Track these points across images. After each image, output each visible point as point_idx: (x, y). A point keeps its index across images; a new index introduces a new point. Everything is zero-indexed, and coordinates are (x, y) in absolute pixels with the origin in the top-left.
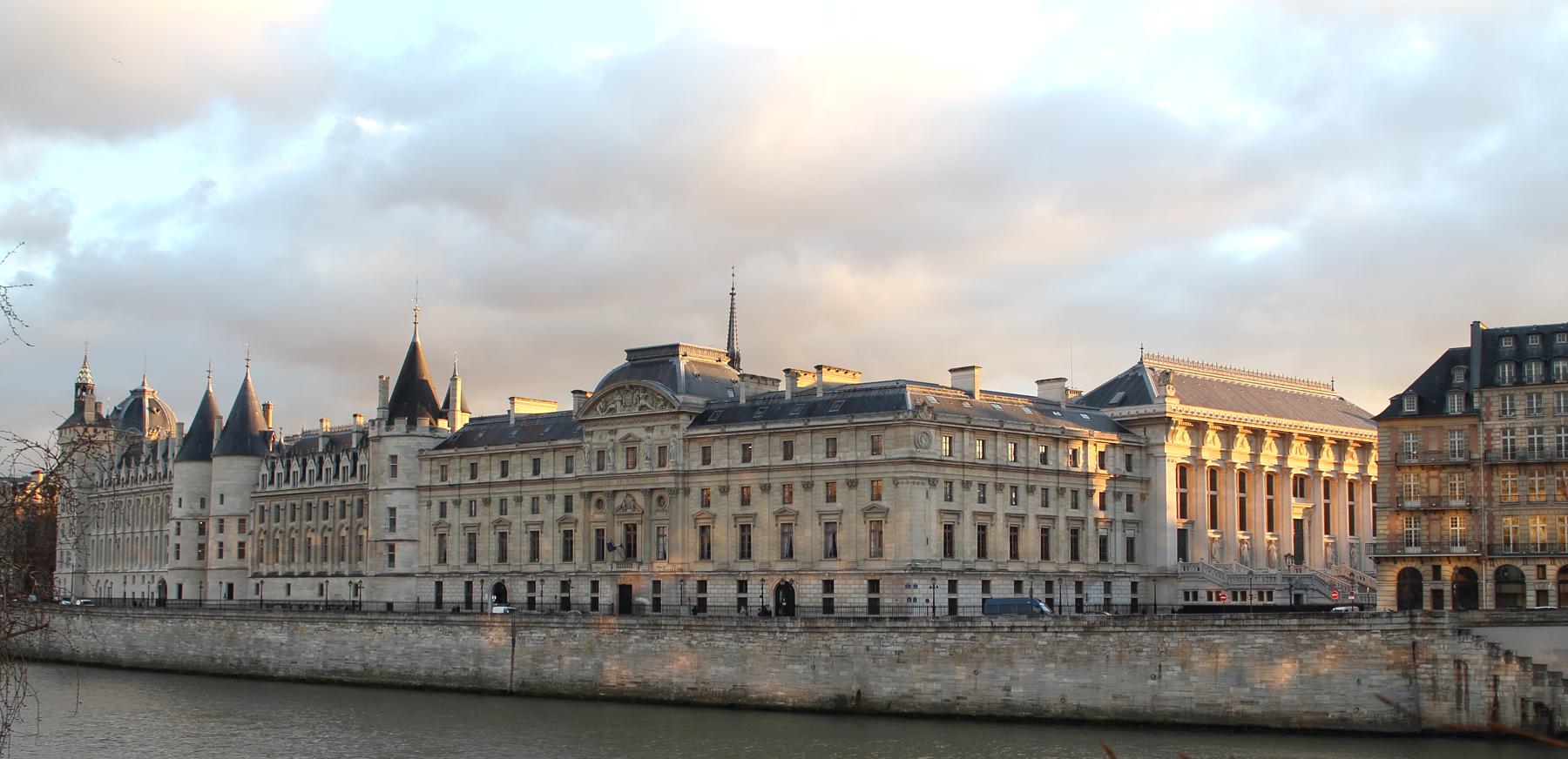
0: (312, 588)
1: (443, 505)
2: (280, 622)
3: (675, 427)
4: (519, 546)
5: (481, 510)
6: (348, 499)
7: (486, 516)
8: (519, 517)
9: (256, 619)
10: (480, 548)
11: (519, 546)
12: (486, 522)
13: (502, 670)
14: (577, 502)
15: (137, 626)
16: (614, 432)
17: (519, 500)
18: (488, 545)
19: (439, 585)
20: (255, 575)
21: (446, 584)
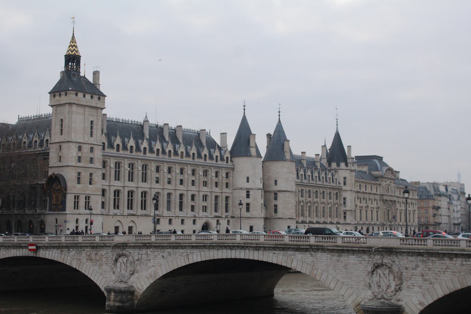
3: (394, 183)
5: (362, 201)
6: (332, 191)
12: (364, 207)
16: (386, 181)
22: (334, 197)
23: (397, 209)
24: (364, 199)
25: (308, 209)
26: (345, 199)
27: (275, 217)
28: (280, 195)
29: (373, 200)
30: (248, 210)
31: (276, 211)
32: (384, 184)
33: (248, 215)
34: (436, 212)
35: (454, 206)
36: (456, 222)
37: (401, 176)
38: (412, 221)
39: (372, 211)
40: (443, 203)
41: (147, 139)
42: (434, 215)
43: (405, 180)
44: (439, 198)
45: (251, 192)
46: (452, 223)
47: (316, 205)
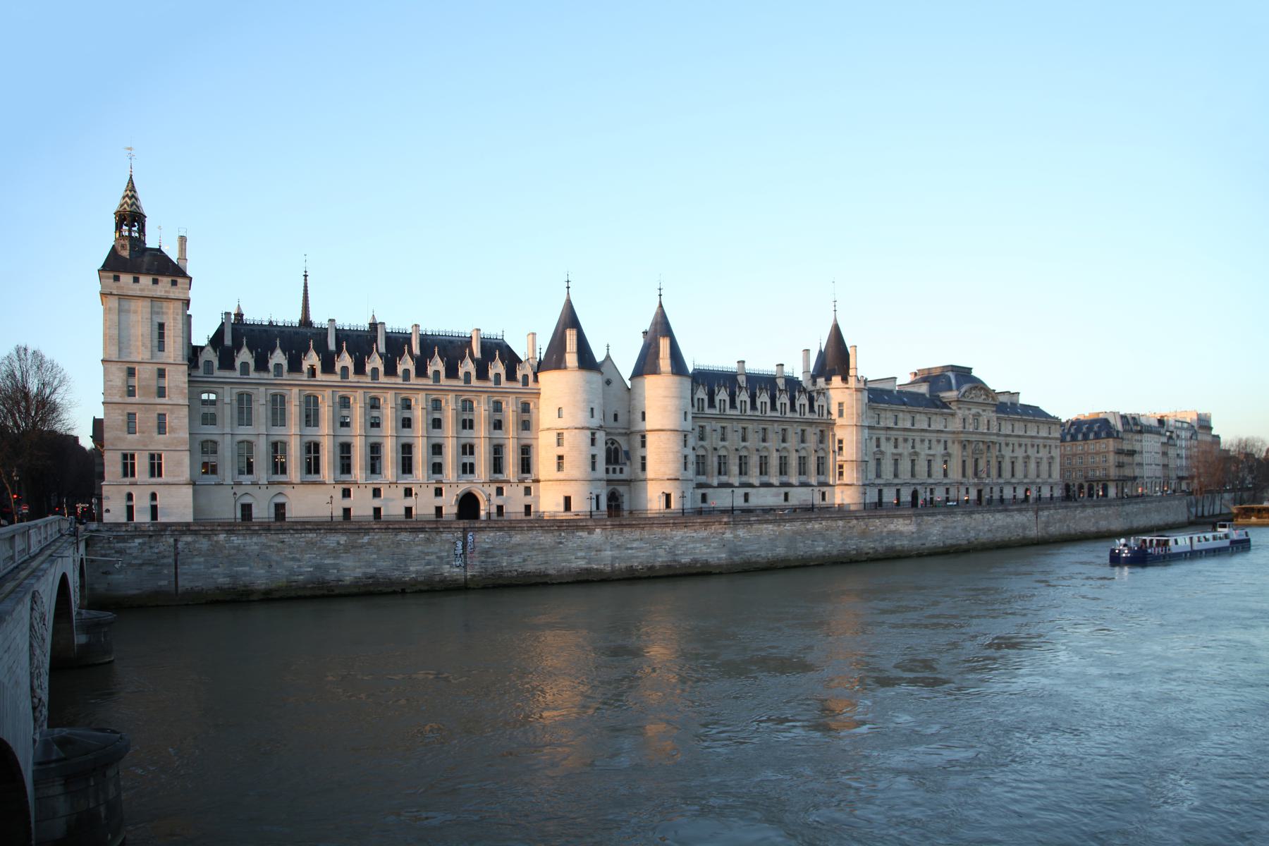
0: (777, 495)
1: (878, 440)
2: (909, 517)
4: (922, 467)
7: (905, 449)
8: (923, 450)
9: (888, 516)
10: (901, 468)
11: (922, 467)
12: (906, 453)
13: (1033, 532)
14: (949, 444)
15: (741, 533)
17: (922, 441)
18: (905, 466)
19: (880, 491)
20: (700, 486)
21: (885, 491)
22: (812, 439)
23: (1003, 457)
24: (906, 440)
25: (737, 461)
26: (840, 442)
27: (642, 477)
28: (650, 438)
29: (934, 443)
30: (560, 467)
31: (644, 468)
32: (960, 413)
33: (561, 475)
34: (1126, 459)
35: (1181, 447)
36: (1185, 474)
37: (1023, 400)
38: (1044, 475)
39: (929, 461)
40: (1150, 444)
41: (381, 356)
42: (1120, 465)
43: (1037, 408)
44: (1137, 437)
45: (566, 435)
46: (1173, 475)
47: (764, 454)
